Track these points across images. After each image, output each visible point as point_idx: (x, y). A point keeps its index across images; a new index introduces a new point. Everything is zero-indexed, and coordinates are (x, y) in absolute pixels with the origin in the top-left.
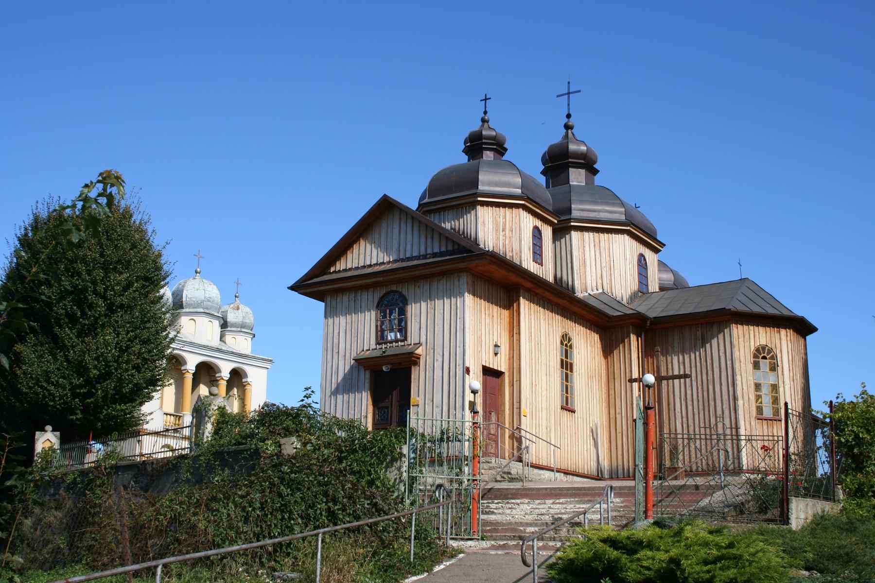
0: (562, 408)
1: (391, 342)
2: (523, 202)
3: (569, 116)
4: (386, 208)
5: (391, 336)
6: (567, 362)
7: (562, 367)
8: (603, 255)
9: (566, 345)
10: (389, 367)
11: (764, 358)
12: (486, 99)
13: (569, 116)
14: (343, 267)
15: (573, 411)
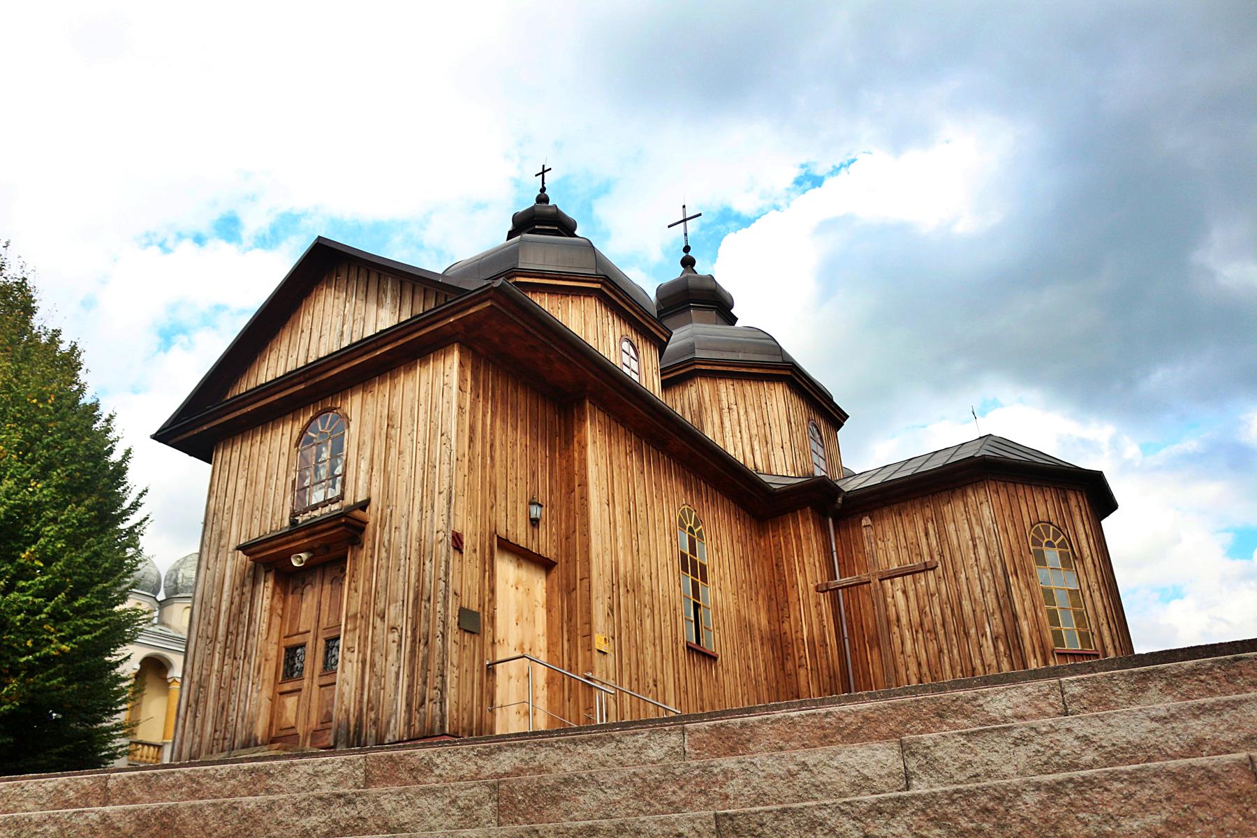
0: (689, 648)
1: (315, 507)
2: (598, 286)
3: (687, 249)
4: (326, 265)
5: (317, 496)
6: (694, 562)
7: (685, 568)
8: (752, 416)
9: (691, 530)
10: (304, 556)
11: (1050, 544)
12: (544, 172)
13: (687, 249)
14: (252, 386)
15: (712, 658)
